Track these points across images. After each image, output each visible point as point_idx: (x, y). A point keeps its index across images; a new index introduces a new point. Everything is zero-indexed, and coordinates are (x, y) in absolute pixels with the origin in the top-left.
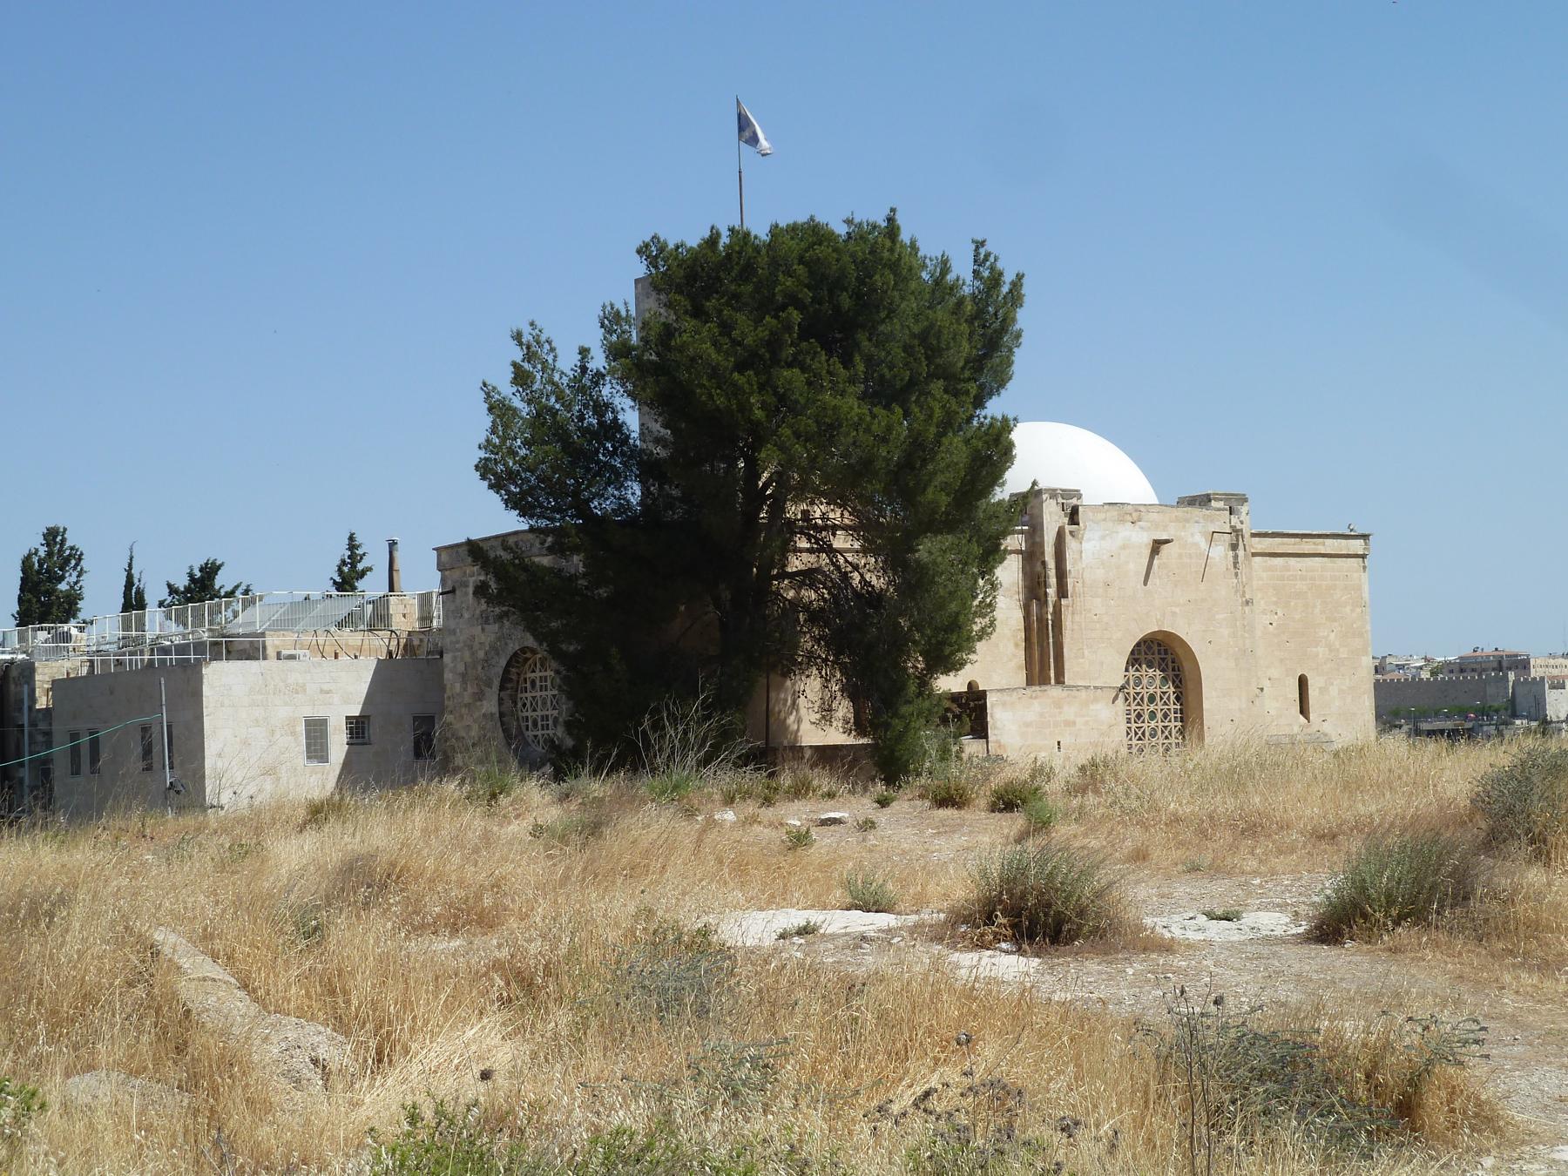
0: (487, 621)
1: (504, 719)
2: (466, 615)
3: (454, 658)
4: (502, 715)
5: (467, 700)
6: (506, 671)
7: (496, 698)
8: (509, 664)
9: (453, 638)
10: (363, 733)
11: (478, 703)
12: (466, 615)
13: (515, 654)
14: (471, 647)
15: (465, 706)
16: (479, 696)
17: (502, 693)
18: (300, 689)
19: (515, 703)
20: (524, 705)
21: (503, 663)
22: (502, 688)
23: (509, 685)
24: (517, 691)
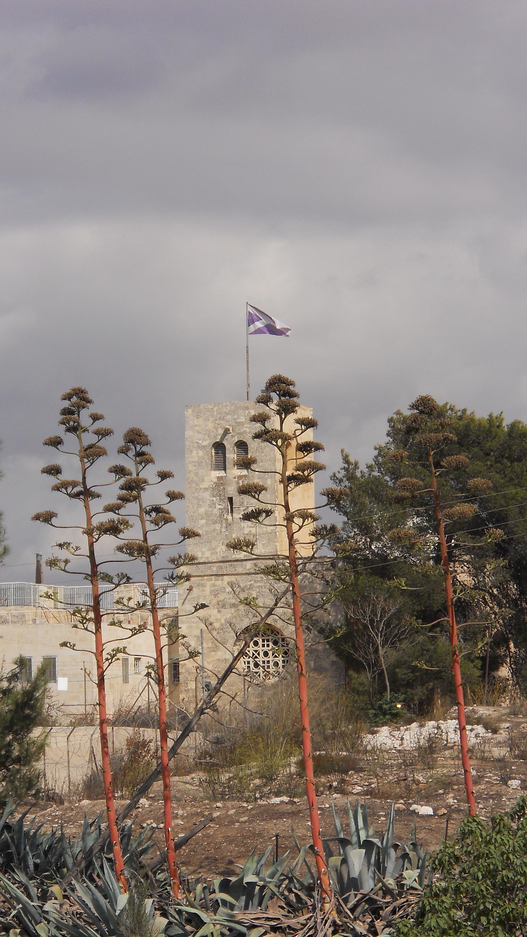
0: (224, 606)
11: (213, 653)
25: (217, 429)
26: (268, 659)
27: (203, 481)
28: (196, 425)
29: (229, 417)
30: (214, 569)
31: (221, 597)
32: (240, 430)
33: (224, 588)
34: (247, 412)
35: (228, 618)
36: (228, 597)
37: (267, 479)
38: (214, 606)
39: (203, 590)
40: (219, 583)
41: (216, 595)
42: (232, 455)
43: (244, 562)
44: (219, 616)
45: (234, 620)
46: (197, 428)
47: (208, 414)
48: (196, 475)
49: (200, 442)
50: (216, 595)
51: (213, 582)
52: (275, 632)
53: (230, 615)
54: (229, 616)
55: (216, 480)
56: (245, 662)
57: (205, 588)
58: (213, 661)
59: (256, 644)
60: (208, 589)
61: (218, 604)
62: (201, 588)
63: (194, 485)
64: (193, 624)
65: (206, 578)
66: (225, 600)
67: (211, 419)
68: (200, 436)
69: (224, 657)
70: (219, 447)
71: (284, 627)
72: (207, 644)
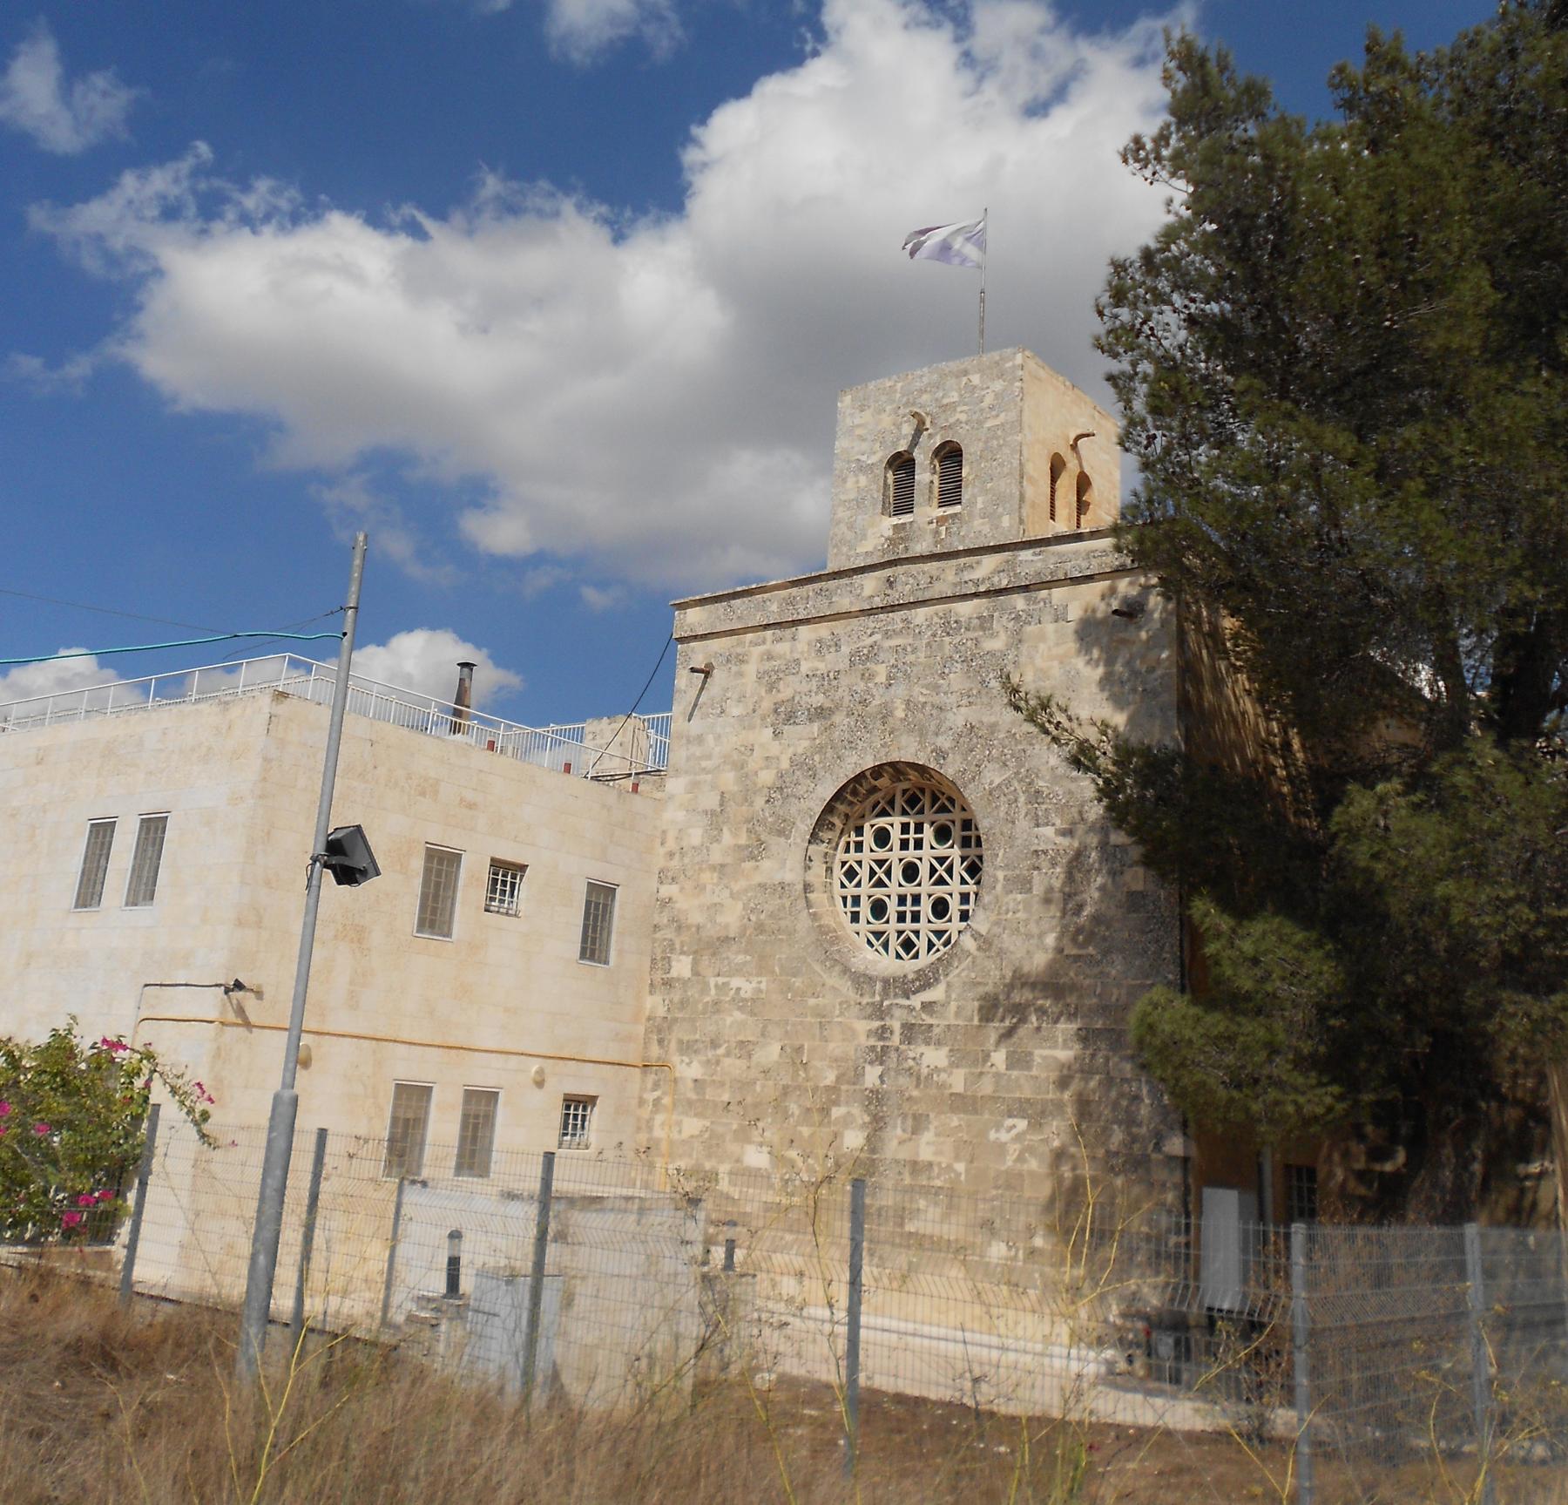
0: (790, 718)
2: (736, 710)
3: (694, 786)
4: (807, 888)
5: (717, 855)
7: (800, 855)
8: (838, 796)
9: (696, 750)
11: (749, 865)
12: (736, 710)
13: (860, 777)
14: (739, 766)
15: (713, 868)
16: (755, 851)
17: (812, 847)
18: (428, 789)
19: (829, 870)
20: (851, 874)
21: (827, 790)
22: (814, 838)
23: (825, 835)
24: (836, 849)
25: (899, 427)
26: (916, 890)
27: (864, 537)
28: (859, 426)
29: (925, 397)
30: (773, 607)
31: (786, 692)
32: (947, 420)
33: (797, 662)
34: (964, 380)
35: (800, 750)
36: (804, 687)
37: (1000, 516)
39: (740, 674)
40: (783, 648)
41: (771, 687)
42: (926, 476)
43: (857, 579)
44: (775, 748)
45: (817, 758)
46: (859, 431)
47: (884, 398)
48: (851, 527)
49: (864, 458)
50: (771, 687)
51: (768, 646)
52: (943, 800)
53: (806, 743)
55: (891, 533)
56: (844, 899)
57: (744, 667)
58: (746, 891)
59: (882, 838)
60: (751, 669)
61: (776, 711)
62: (734, 669)
63: (845, 549)
64: (702, 777)
65: (750, 636)
66: (797, 699)
67: (888, 408)
68: (865, 446)
69: (778, 878)
70: (902, 464)
71: (969, 776)
72: (735, 835)
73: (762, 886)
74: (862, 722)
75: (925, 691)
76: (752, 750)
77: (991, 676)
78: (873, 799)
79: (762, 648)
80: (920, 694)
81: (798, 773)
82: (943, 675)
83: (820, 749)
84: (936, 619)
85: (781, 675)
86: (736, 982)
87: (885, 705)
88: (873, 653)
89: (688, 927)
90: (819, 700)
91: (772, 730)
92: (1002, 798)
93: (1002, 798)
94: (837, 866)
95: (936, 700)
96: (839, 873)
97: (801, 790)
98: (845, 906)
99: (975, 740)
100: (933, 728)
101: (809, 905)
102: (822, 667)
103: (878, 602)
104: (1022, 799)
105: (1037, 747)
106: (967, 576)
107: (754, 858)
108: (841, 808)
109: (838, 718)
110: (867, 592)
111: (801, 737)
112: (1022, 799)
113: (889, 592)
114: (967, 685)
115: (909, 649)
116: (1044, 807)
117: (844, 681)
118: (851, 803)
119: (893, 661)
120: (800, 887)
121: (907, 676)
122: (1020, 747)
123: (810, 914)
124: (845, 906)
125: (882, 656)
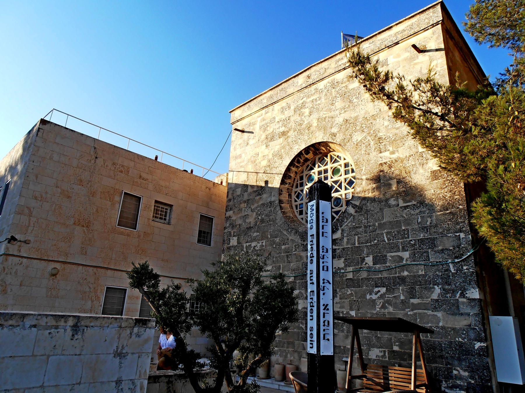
0: (272, 139)
1: (282, 205)
4: (281, 202)
6: (288, 169)
8: (292, 164)
10: (166, 216)
13: (300, 154)
15: (245, 202)
19: (290, 196)
23: (288, 181)
24: (292, 187)
31: (270, 130)
33: (274, 118)
35: (276, 150)
38: (262, 142)
41: (265, 130)
44: (266, 152)
53: (278, 147)
54: (277, 148)
56: (296, 206)
57: (255, 126)
58: (257, 208)
61: (267, 138)
66: (274, 132)
69: (269, 200)
71: (346, 140)
73: (263, 205)
74: (300, 133)
75: (325, 113)
76: (258, 155)
77: (354, 98)
78: (306, 164)
79: (261, 117)
80: (323, 114)
81: (275, 158)
82: (332, 104)
83: (283, 147)
84: (328, 84)
85: (268, 125)
86: (253, 244)
87: (309, 123)
88: (303, 105)
89: (236, 226)
90: (282, 129)
91: (265, 145)
92: (363, 145)
93: (363, 145)
94: (293, 194)
95: (330, 114)
96: (294, 197)
97: (277, 164)
98: (297, 209)
99: (348, 125)
100: (329, 126)
101: (281, 208)
102: (283, 117)
103: (304, 85)
104: (372, 143)
105: (378, 120)
106: (340, 63)
107: (260, 195)
108: (294, 169)
109: (291, 133)
110: (300, 83)
111: (277, 145)
112: (372, 143)
113: (309, 80)
114: (343, 105)
115: (318, 99)
116: (383, 144)
117: (292, 119)
118: (297, 167)
119: (311, 106)
120: (277, 202)
121: (318, 109)
122: (369, 122)
123: (282, 212)
124: (297, 209)
125: (307, 105)
